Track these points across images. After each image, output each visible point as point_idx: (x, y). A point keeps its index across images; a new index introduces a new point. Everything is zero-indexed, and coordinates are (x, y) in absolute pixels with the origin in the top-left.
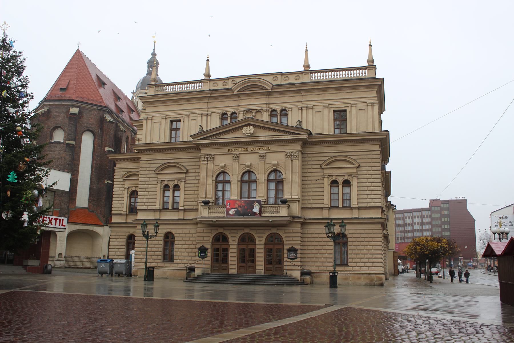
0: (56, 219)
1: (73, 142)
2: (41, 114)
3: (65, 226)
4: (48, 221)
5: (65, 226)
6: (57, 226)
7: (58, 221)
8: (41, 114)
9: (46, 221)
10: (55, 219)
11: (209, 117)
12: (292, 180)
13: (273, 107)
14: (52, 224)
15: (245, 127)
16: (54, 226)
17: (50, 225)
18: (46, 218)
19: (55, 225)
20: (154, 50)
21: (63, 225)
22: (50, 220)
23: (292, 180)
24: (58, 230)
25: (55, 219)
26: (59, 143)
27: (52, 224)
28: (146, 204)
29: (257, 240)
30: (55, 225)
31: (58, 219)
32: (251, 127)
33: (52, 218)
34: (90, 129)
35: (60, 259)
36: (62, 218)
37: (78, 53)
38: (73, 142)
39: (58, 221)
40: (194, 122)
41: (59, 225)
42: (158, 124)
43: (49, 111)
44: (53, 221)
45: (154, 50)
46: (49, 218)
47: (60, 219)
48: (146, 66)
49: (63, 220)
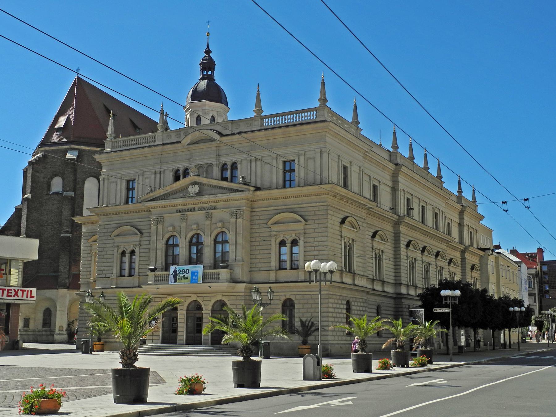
0: (23, 291)
1: (72, 194)
2: (34, 161)
3: (33, 297)
4: (13, 293)
5: (33, 297)
6: (25, 298)
7: (25, 293)
8: (34, 161)
9: (11, 293)
10: (21, 290)
11: (162, 175)
12: (236, 242)
13: (223, 160)
14: (18, 296)
15: (190, 187)
16: (20, 298)
17: (16, 297)
18: (11, 290)
19: (22, 296)
20: (208, 45)
21: (31, 297)
22: (16, 293)
23: (236, 242)
24: (23, 302)
25: (21, 290)
26: (57, 193)
27: (18, 296)
28: (105, 272)
29: (204, 308)
30: (22, 296)
31: (25, 291)
32: (197, 186)
33: (18, 290)
34: (93, 174)
35: (61, 332)
36: (29, 289)
37: (79, 80)
38: (72, 194)
39: (25, 293)
40: (147, 181)
41: (27, 297)
42: (114, 184)
43: (44, 157)
44: (20, 293)
45: (208, 45)
46: (15, 290)
47: (28, 291)
48: (198, 68)
49: (31, 291)
